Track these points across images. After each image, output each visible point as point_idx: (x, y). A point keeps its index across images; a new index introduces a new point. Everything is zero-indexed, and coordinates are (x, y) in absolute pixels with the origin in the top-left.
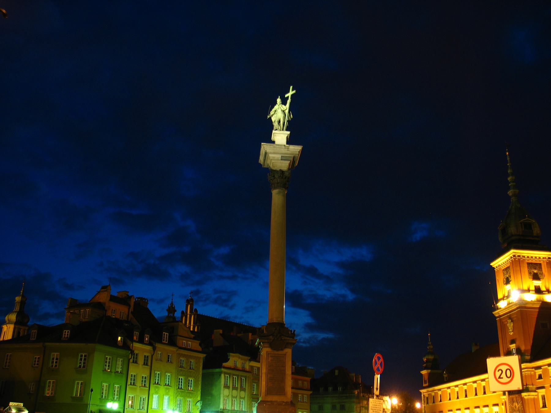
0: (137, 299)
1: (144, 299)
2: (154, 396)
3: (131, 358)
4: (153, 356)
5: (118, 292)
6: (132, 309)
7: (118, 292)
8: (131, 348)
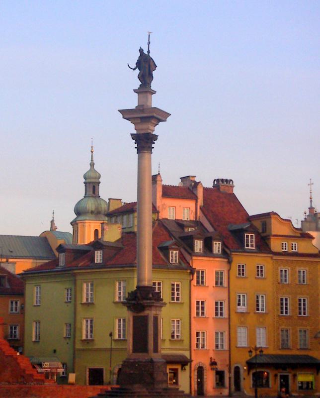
0: (216, 183)
1: (227, 181)
2: (239, 330)
3: (192, 280)
4: (231, 271)
5: (181, 178)
6: (200, 202)
7: (181, 178)
8: (191, 265)
